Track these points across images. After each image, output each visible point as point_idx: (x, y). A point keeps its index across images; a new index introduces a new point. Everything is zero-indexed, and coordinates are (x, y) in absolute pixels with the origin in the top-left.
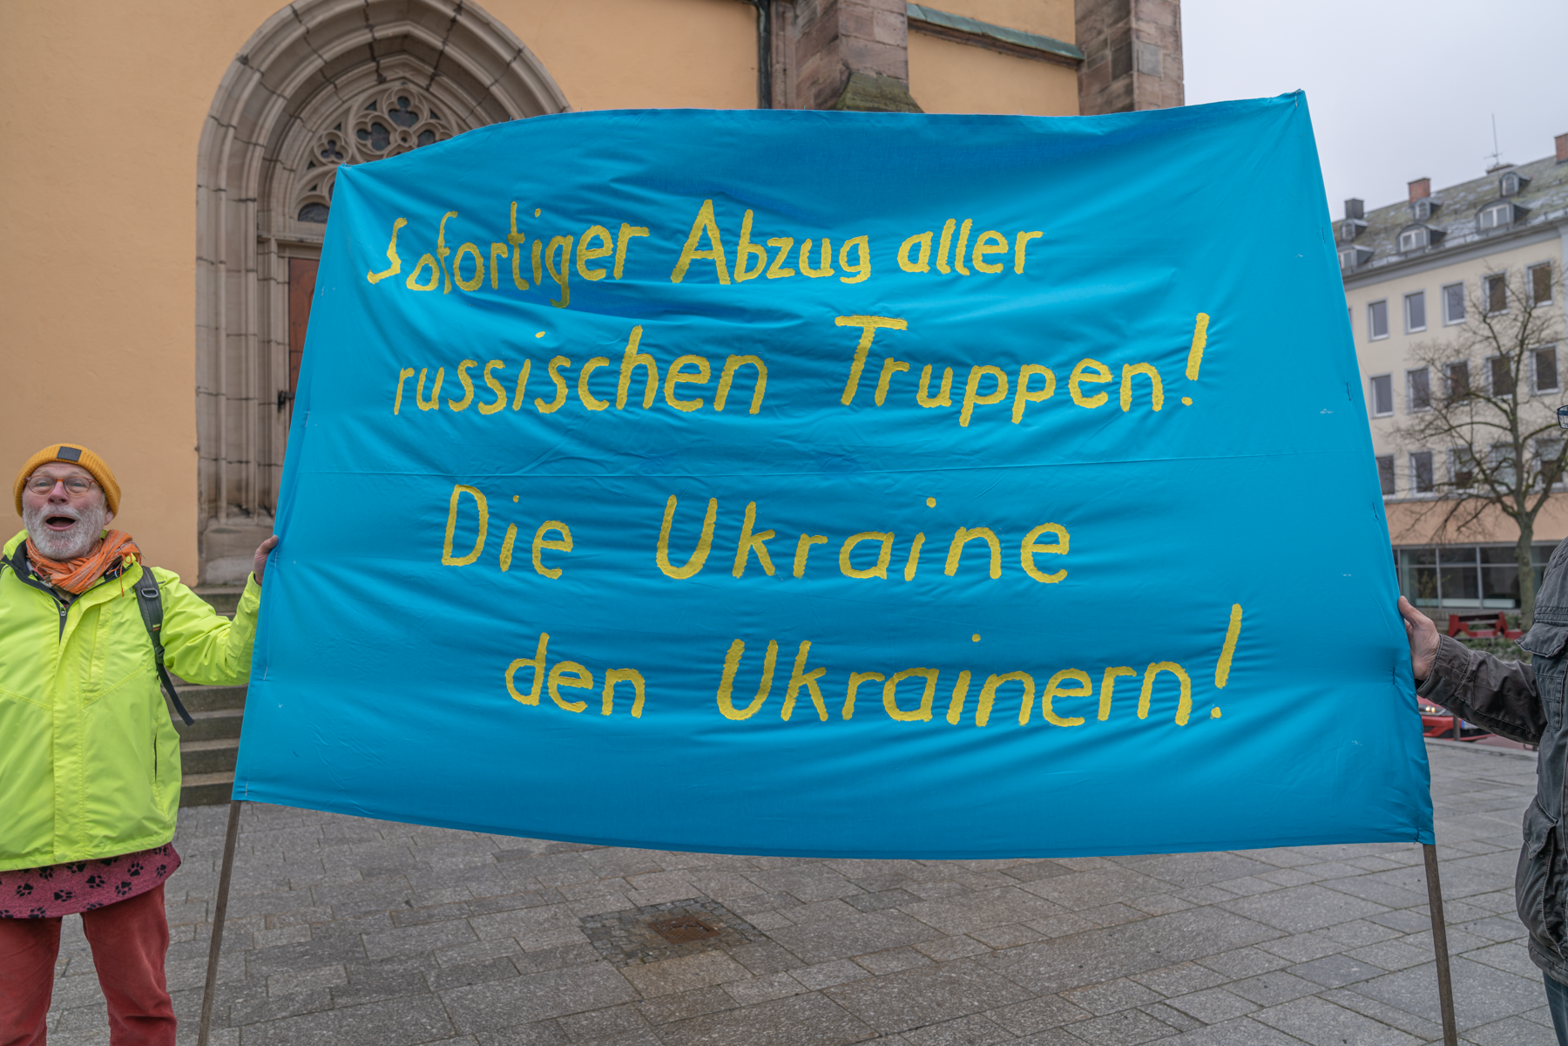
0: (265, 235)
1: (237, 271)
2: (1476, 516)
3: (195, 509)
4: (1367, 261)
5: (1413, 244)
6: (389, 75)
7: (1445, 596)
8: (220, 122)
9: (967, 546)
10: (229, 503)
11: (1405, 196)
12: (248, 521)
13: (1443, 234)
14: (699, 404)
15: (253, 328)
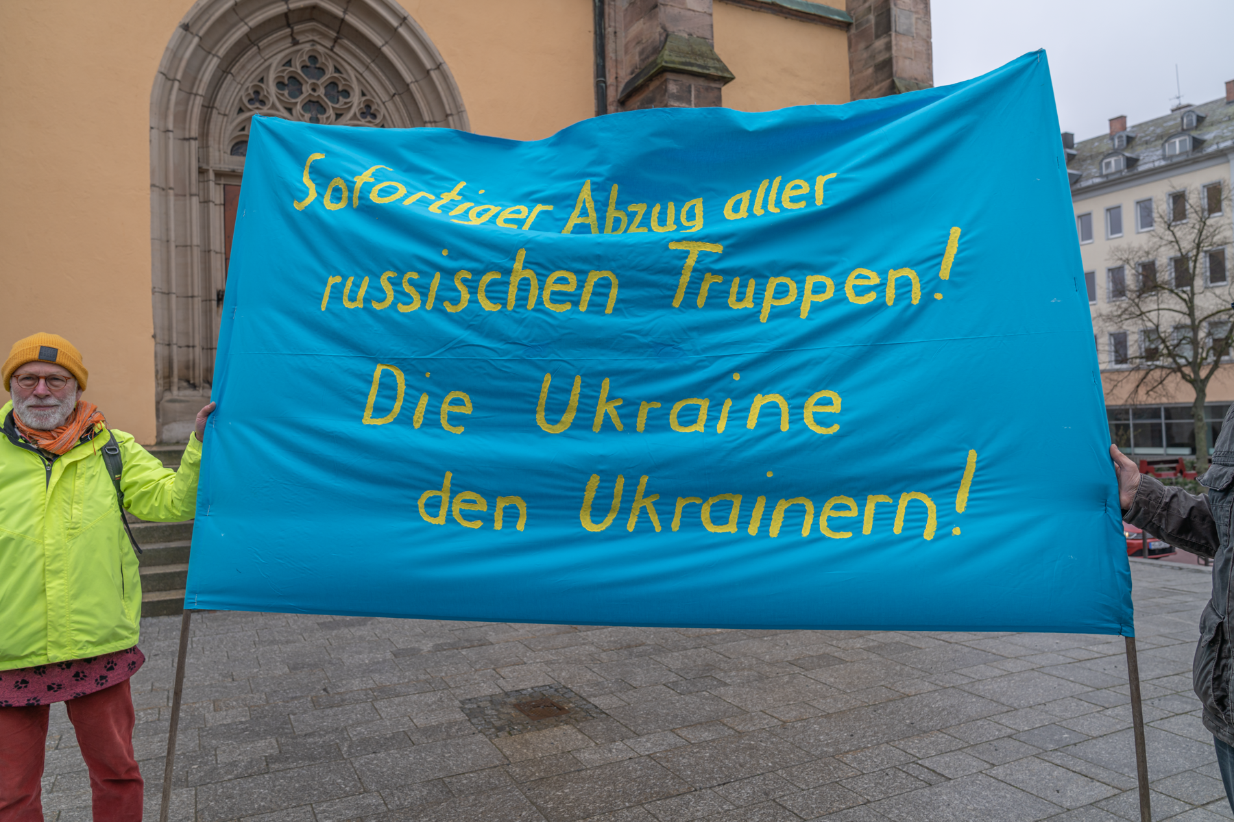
0: (205, 167)
1: (183, 195)
2: (1161, 383)
3: (153, 384)
4: (1076, 182)
5: (1113, 168)
6: (301, 38)
7: (1137, 445)
8: (167, 76)
9: (763, 407)
10: (180, 379)
11: (1106, 130)
13: (1137, 160)
14: (568, 306)
15: (196, 240)
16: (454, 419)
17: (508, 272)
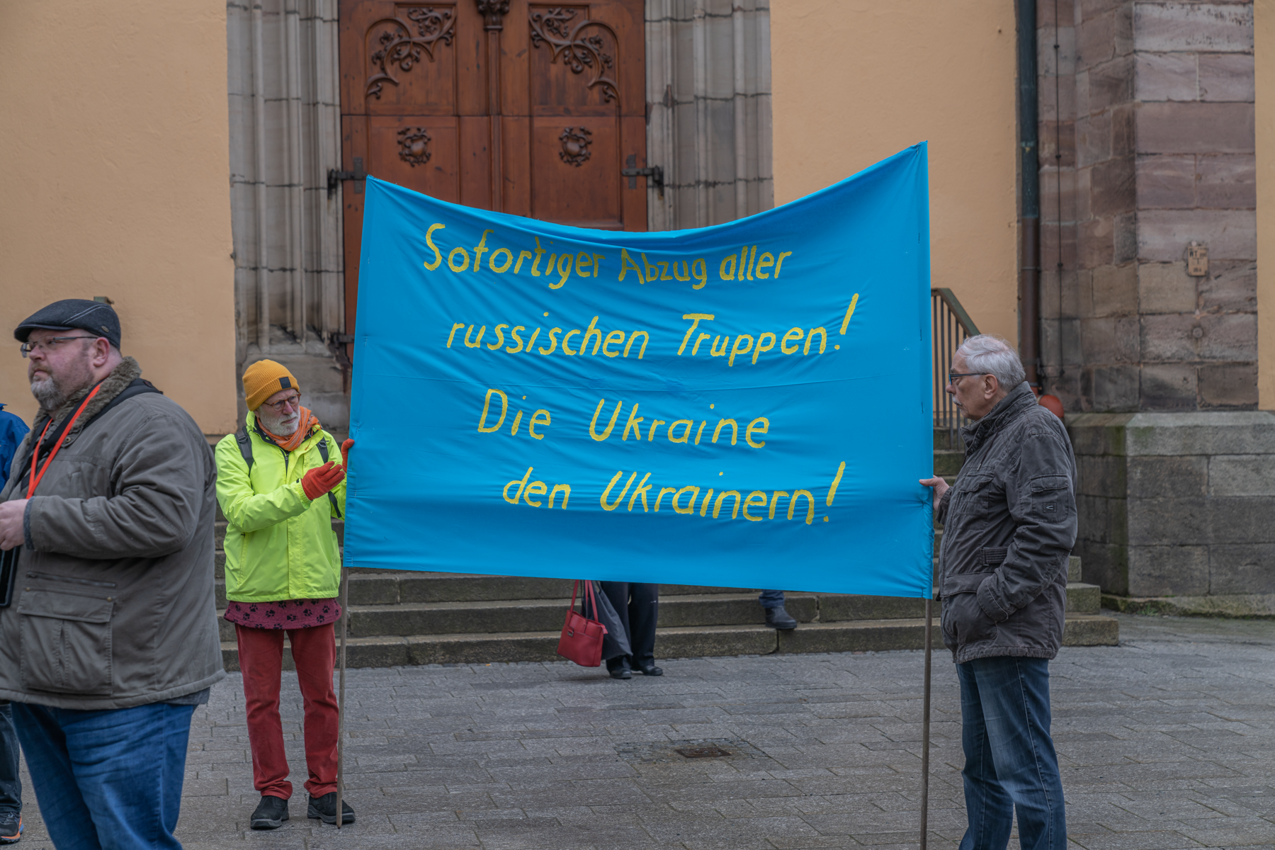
3: (233, 334)
10: (272, 325)
12: (295, 348)
15: (296, 90)
16: (538, 429)
17: (584, 330)
